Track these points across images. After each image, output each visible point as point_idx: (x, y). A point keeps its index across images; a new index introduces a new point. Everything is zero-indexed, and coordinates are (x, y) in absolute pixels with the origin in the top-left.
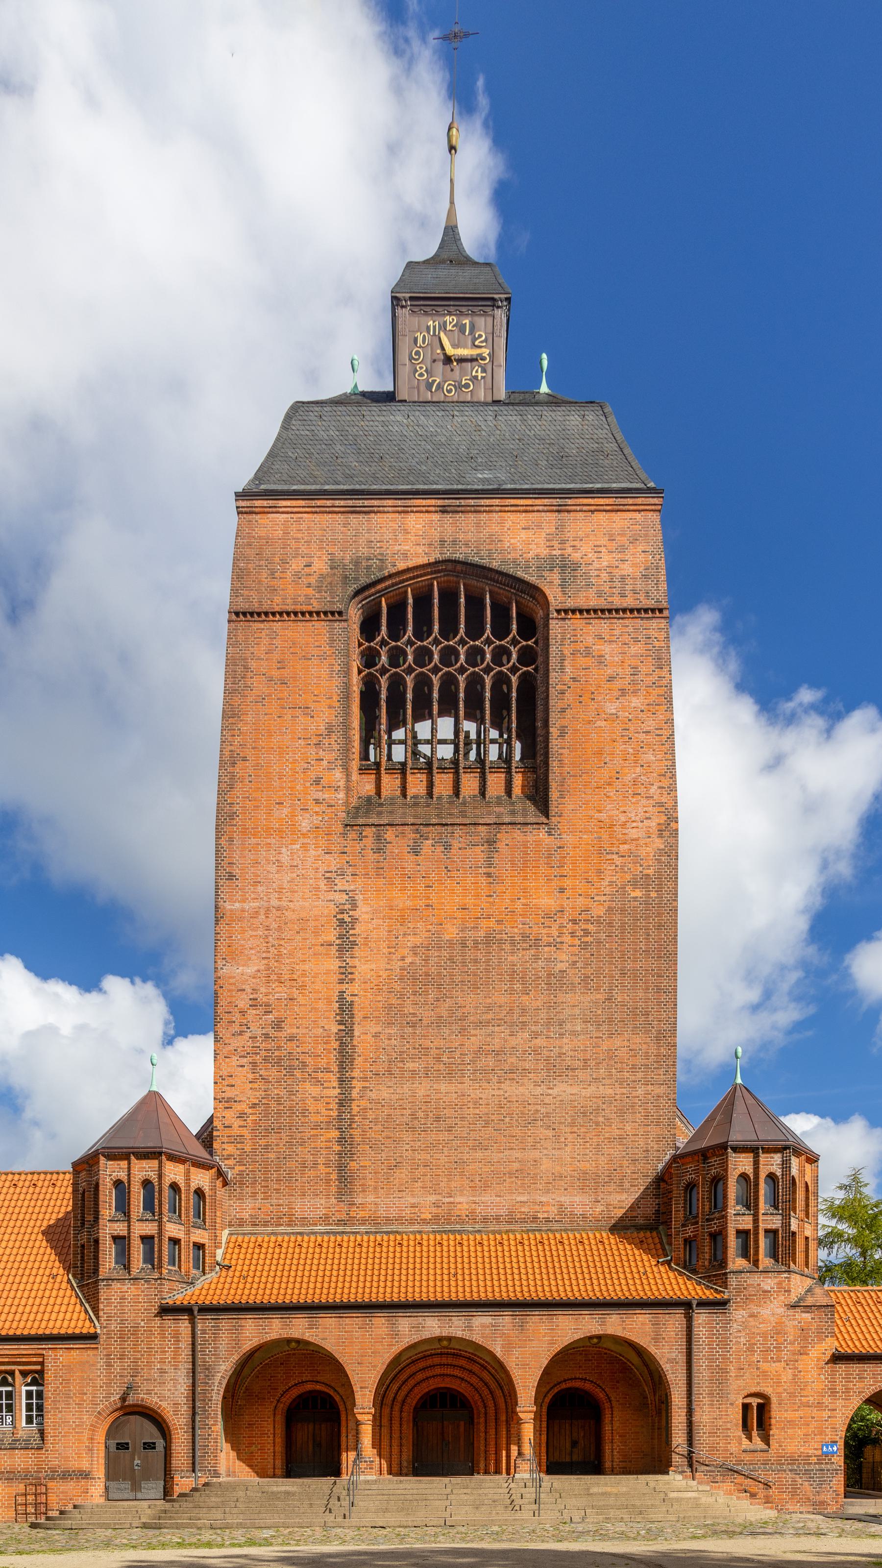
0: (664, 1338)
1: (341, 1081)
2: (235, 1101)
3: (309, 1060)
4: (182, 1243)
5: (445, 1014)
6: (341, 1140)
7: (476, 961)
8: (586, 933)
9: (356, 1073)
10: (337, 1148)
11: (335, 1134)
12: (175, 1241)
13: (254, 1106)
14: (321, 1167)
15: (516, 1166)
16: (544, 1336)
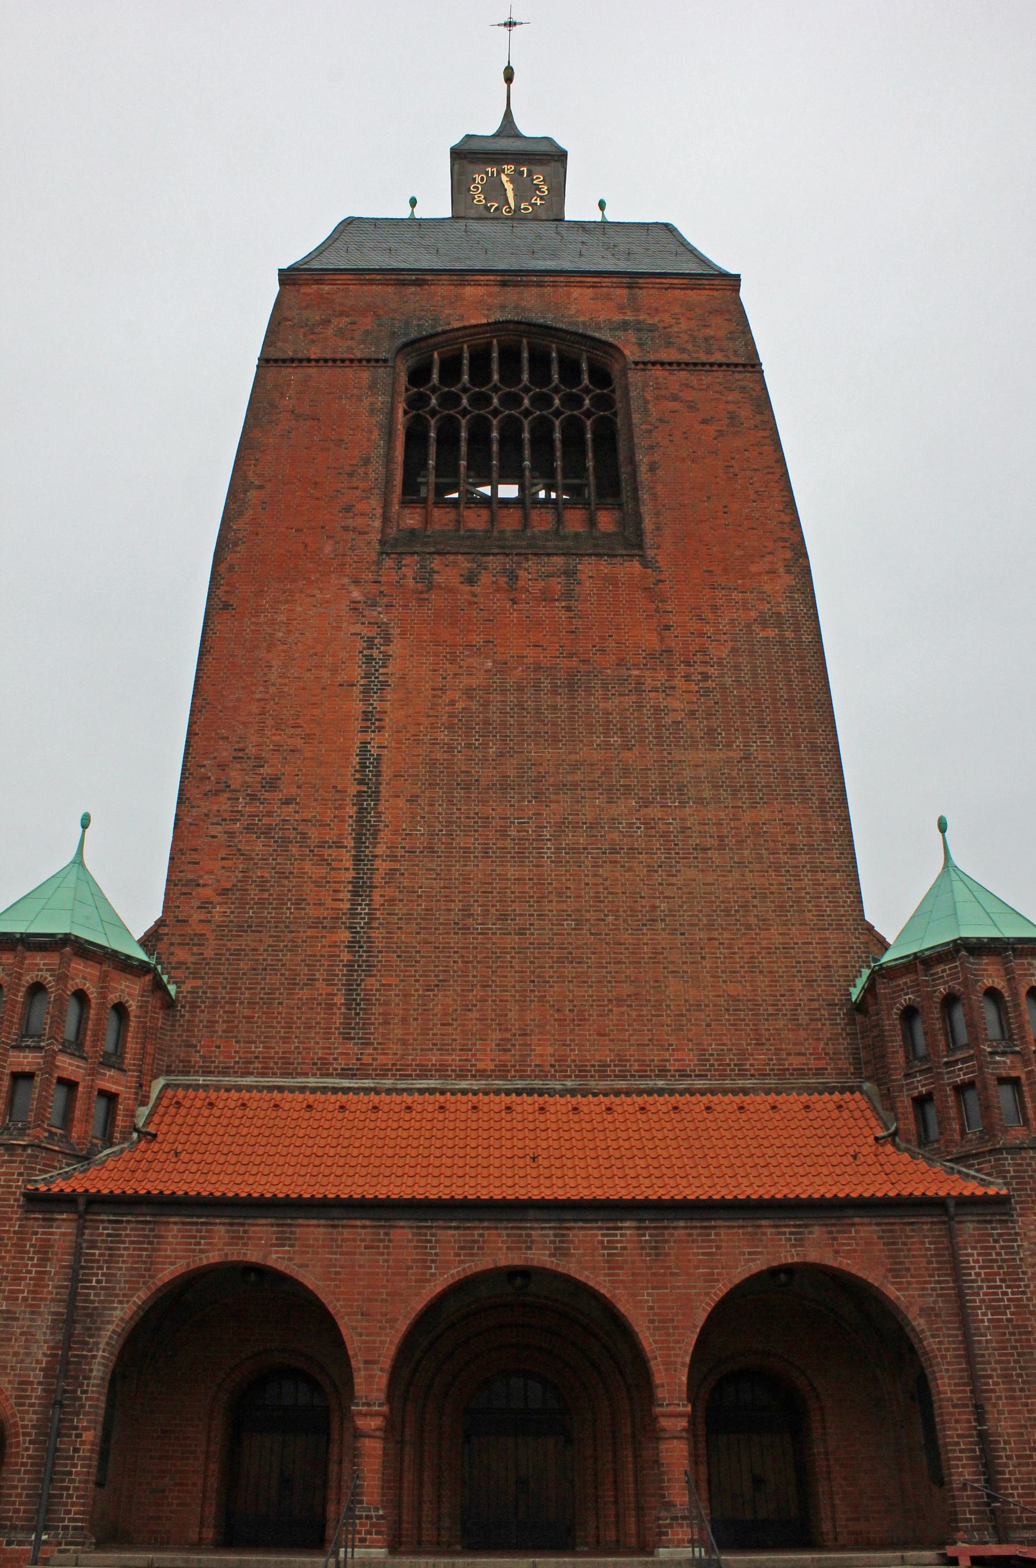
0: (908, 1270)
1: (357, 859)
2: (198, 885)
4: (80, 1089)
5: (512, 773)
7: (554, 708)
8: (705, 677)
9: (380, 850)
10: (346, 956)
12: (69, 1085)
13: (224, 892)
14: (320, 985)
15: (627, 989)
16: (698, 1268)
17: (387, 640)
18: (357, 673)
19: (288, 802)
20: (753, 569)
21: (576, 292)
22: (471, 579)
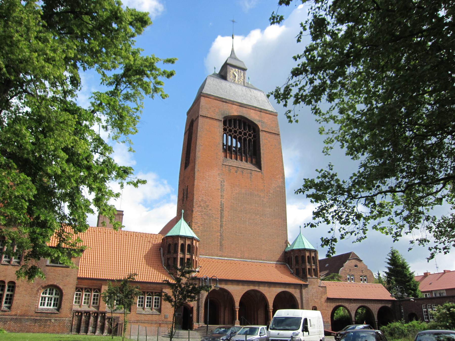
1: (221, 221)
3: (214, 216)
6: (221, 235)
7: (248, 198)
11: (219, 234)
13: (201, 225)
15: (257, 246)
17: (224, 182)
18: (219, 187)
19: (210, 210)
20: (277, 177)
21: (252, 111)
22: (236, 172)
